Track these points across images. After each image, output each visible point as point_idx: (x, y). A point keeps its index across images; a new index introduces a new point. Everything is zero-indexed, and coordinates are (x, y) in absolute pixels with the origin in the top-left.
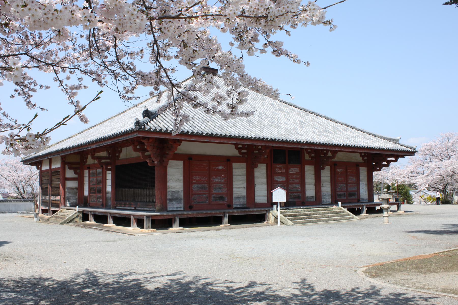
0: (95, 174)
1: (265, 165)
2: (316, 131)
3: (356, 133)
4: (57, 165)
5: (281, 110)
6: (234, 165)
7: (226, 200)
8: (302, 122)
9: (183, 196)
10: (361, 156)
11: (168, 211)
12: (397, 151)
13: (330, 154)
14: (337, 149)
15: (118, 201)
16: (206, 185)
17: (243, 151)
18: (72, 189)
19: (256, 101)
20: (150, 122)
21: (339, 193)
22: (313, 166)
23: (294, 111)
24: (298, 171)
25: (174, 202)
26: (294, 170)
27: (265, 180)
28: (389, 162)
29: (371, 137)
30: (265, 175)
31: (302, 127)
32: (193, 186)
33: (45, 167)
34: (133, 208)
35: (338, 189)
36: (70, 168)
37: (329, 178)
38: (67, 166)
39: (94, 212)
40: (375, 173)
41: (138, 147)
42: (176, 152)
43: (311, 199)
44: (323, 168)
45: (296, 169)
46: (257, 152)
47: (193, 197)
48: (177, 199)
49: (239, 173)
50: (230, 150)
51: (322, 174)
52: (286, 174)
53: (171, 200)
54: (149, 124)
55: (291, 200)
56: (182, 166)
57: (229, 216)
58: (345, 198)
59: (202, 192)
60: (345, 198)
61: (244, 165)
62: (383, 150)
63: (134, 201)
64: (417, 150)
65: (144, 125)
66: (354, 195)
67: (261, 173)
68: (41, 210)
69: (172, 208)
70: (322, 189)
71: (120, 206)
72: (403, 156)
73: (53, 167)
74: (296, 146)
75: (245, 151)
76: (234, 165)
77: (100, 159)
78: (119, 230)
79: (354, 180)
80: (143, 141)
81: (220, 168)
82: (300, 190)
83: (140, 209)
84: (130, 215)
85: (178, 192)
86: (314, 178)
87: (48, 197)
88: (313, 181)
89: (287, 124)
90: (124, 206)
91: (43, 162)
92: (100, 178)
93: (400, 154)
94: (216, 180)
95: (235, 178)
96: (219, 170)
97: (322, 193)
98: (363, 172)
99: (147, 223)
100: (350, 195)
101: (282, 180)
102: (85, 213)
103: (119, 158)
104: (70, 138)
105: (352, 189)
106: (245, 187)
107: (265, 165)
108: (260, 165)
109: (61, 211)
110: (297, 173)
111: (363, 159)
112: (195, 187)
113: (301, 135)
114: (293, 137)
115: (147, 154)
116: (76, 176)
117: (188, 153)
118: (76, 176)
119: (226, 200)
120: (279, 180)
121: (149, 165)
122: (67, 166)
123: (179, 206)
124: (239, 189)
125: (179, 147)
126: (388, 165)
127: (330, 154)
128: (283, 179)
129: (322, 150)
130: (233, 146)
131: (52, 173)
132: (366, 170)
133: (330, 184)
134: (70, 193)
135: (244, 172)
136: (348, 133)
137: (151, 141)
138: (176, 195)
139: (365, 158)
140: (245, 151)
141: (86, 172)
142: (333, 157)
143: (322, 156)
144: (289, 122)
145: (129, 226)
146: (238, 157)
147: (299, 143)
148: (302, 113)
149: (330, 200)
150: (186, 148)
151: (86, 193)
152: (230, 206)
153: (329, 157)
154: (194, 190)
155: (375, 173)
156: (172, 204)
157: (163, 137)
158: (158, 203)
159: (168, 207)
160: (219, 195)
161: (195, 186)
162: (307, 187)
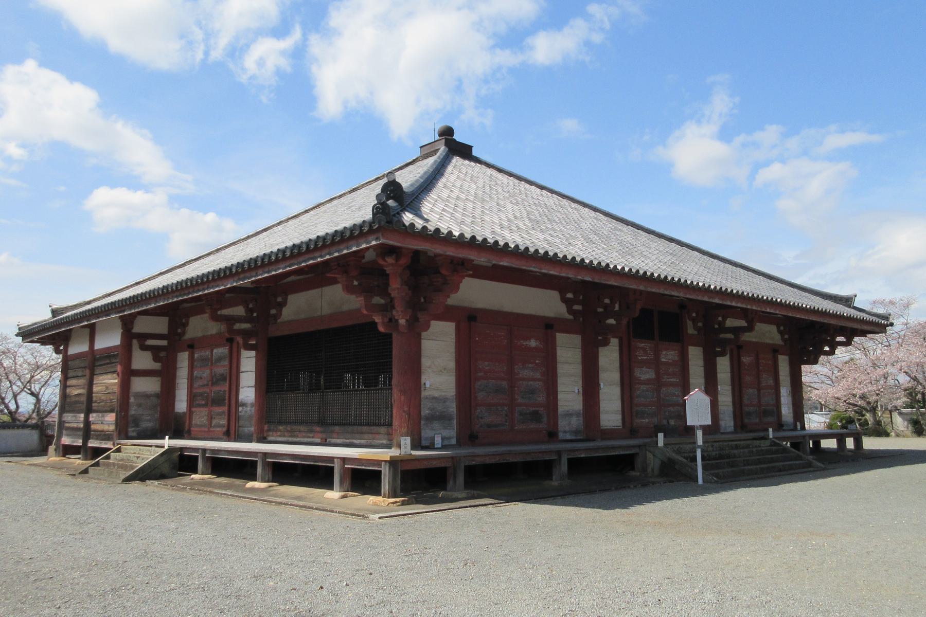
0: (208, 362)
4: (109, 340)
5: (616, 229)
7: (545, 419)
9: (454, 410)
15: (269, 422)
18: (147, 396)
24: (676, 358)
25: (436, 425)
26: (669, 355)
28: (834, 346)
30: (618, 365)
33: (78, 348)
36: (144, 348)
37: (729, 375)
38: (135, 343)
39: (214, 451)
40: (805, 368)
45: (673, 352)
50: (546, 303)
52: (656, 363)
53: (431, 419)
56: (453, 337)
57: (570, 460)
60: (757, 421)
72: (863, 333)
78: (299, 498)
79: (771, 382)
81: (533, 343)
84: (331, 459)
85: (444, 400)
86: (702, 374)
87: (82, 415)
91: (73, 335)
92: (222, 369)
93: (865, 327)
94: (525, 373)
96: (530, 349)
106: (581, 390)
109: (118, 450)
116: (157, 366)
117: (466, 304)
118: (157, 366)
119: (545, 419)
121: (381, 329)
122: (135, 343)
126: (832, 353)
134: (140, 405)
141: (183, 359)
145: (329, 486)
146: (567, 320)
149: (732, 424)
151: (181, 405)
154: (481, 396)
155: (805, 368)
156: (432, 429)
158: (401, 427)
160: (531, 409)
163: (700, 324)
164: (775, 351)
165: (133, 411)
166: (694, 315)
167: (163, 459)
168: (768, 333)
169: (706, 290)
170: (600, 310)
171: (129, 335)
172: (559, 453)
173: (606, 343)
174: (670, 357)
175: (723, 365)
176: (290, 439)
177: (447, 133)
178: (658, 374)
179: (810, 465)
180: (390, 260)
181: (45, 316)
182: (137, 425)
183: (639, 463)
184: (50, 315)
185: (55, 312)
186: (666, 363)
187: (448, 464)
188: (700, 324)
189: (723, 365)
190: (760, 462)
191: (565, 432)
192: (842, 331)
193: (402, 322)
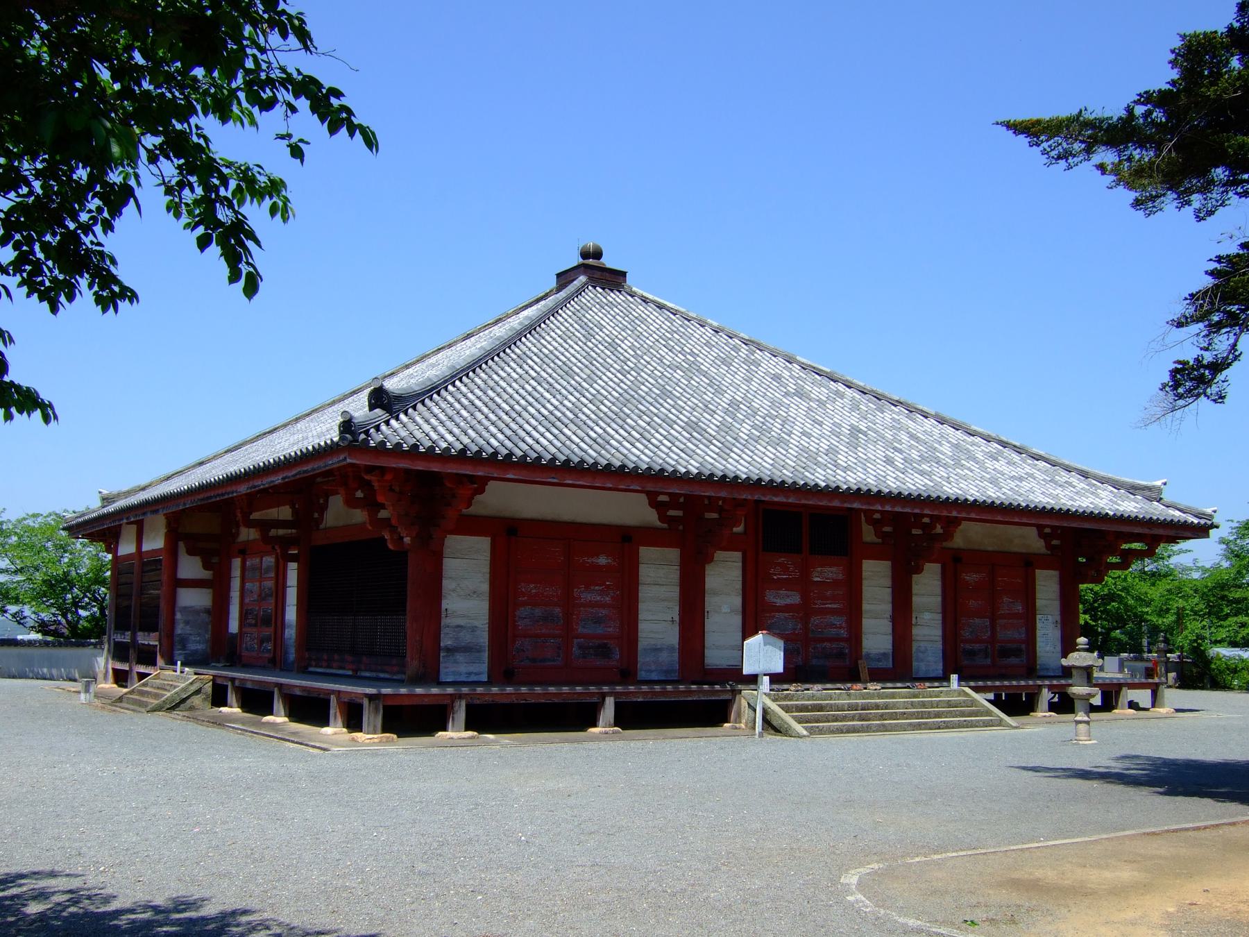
1: (737, 555)
2: (898, 458)
3: (1026, 467)
4: (155, 542)
5: (800, 393)
6: (645, 552)
8: (860, 431)
10: (1041, 535)
11: (440, 684)
12: (1151, 523)
13: (939, 529)
14: (954, 514)
15: (317, 649)
16: (557, 610)
17: (671, 513)
19: (729, 365)
20: (387, 423)
21: (968, 646)
22: (888, 563)
23: (842, 397)
24: (841, 577)
25: (460, 657)
26: (827, 573)
27: (737, 601)
29: (1074, 479)
30: (739, 586)
31: (853, 445)
32: (517, 613)
33: (127, 548)
34: (350, 673)
35: (966, 634)
36: (191, 552)
37: (939, 599)
38: (181, 545)
41: (359, 494)
42: (472, 510)
43: (879, 660)
44: (919, 570)
45: (834, 569)
46: (715, 516)
47: (518, 643)
48: (467, 649)
49: (658, 576)
50: (632, 510)
52: (803, 584)
53: (449, 650)
54: (383, 427)
55: (814, 662)
56: (488, 554)
58: (989, 661)
60: (989, 661)
61: (673, 554)
62: (1103, 518)
64: (1215, 521)
65: (367, 433)
66: (1017, 652)
67: (724, 579)
68: (111, 671)
69: (454, 673)
70: (915, 631)
71: (316, 666)
72: (1173, 540)
73: (146, 547)
74: (824, 503)
75: (679, 513)
76: (645, 552)
77: (264, 526)
78: (294, 734)
79: (1019, 608)
80: (367, 477)
81: (602, 560)
82: (844, 633)
83: (367, 674)
85: (474, 629)
86: (890, 599)
88: (887, 608)
89: (808, 436)
90: (328, 667)
91: (123, 532)
93: (1161, 532)
94: (588, 597)
95: (645, 592)
96: (599, 568)
97: (915, 646)
98: (1047, 587)
99: (371, 717)
100: (1005, 653)
101: (788, 601)
102: (219, 681)
103: (322, 526)
104: (201, 464)
105: (1011, 633)
106: (677, 618)
107: (737, 555)
108: (719, 555)
109: (157, 677)
110: (835, 583)
111: (1048, 546)
113: (845, 469)
114: (819, 477)
115: (383, 514)
116: (206, 574)
117: (507, 514)
118: (206, 574)
120: (780, 602)
121: (391, 547)
122: (181, 545)
123: (472, 669)
124: (658, 623)
125: (478, 497)
127: (939, 529)
128: (794, 598)
129: (915, 515)
130: (643, 498)
131: (144, 564)
132: (1056, 579)
133: (939, 617)
134: (187, 623)
135: (674, 574)
136: (1001, 465)
137: (388, 477)
138: (466, 638)
139: (1055, 542)
140: (679, 513)
141: (237, 563)
142: (948, 535)
143: (914, 532)
144: (816, 432)
145: (324, 722)
146: (655, 529)
147: (833, 492)
148: (866, 404)
150: (503, 498)
151: (234, 626)
152: (627, 674)
153: (936, 538)
154: (521, 624)
156: (456, 662)
157: (420, 466)
159: (443, 670)
161: (524, 611)
162: (867, 623)
165: (180, 629)
171: (173, 537)
176: (341, 672)
178: (805, 596)
182: (184, 648)
185: (106, 500)
188: (887, 529)
190: (911, 716)
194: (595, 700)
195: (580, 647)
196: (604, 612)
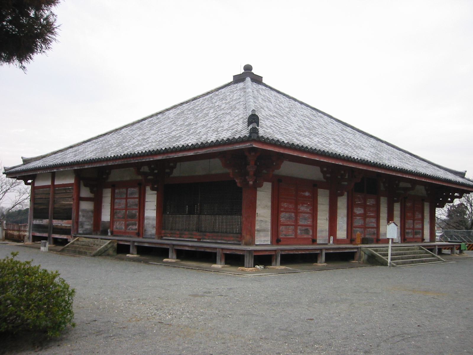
5: (343, 130)
6: (320, 191)
26: (371, 202)
28: (453, 198)
34: (196, 240)
36: (86, 185)
40: (437, 209)
45: (372, 200)
48: (264, 230)
50: (313, 173)
51: (395, 208)
52: (364, 206)
53: (258, 231)
56: (271, 190)
57: (326, 254)
59: (289, 223)
60: (412, 236)
61: (327, 192)
63: (198, 230)
71: (171, 237)
73: (56, 183)
76: (320, 191)
79: (420, 216)
81: (307, 194)
82: (375, 226)
85: (266, 222)
90: (180, 237)
96: (306, 197)
99: (249, 260)
106: (328, 219)
112: (284, 217)
116: (91, 195)
118: (91, 195)
119: (311, 234)
121: (239, 185)
130: (318, 168)
134: (83, 216)
145: (215, 262)
151: (106, 217)
155: (437, 209)
160: (304, 228)
163: (387, 185)
164: (423, 200)
165: (81, 219)
166: (384, 180)
167: (109, 246)
168: (421, 190)
169: (395, 169)
170: (339, 177)
172: (321, 250)
173: (342, 195)
174: (372, 202)
175: (397, 208)
177: (248, 68)
178: (365, 211)
179: (439, 260)
180: (253, 154)
181: (16, 162)
182: (82, 227)
183: (357, 255)
184: (21, 162)
185: (26, 161)
186: (369, 206)
187: (273, 253)
189: (397, 208)
191: (320, 240)
192: (457, 190)
193: (251, 183)
194: (318, 252)
195: (300, 230)
196: (307, 215)
